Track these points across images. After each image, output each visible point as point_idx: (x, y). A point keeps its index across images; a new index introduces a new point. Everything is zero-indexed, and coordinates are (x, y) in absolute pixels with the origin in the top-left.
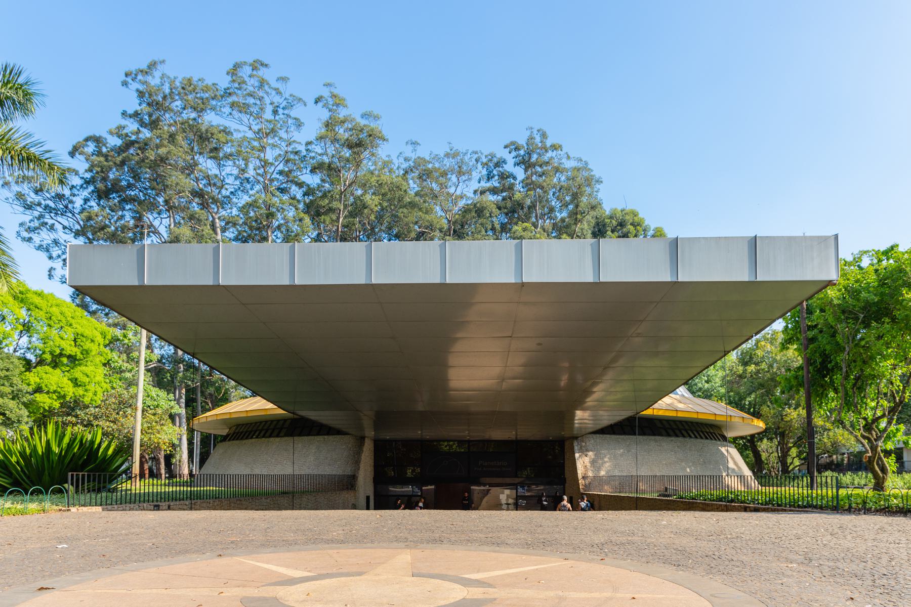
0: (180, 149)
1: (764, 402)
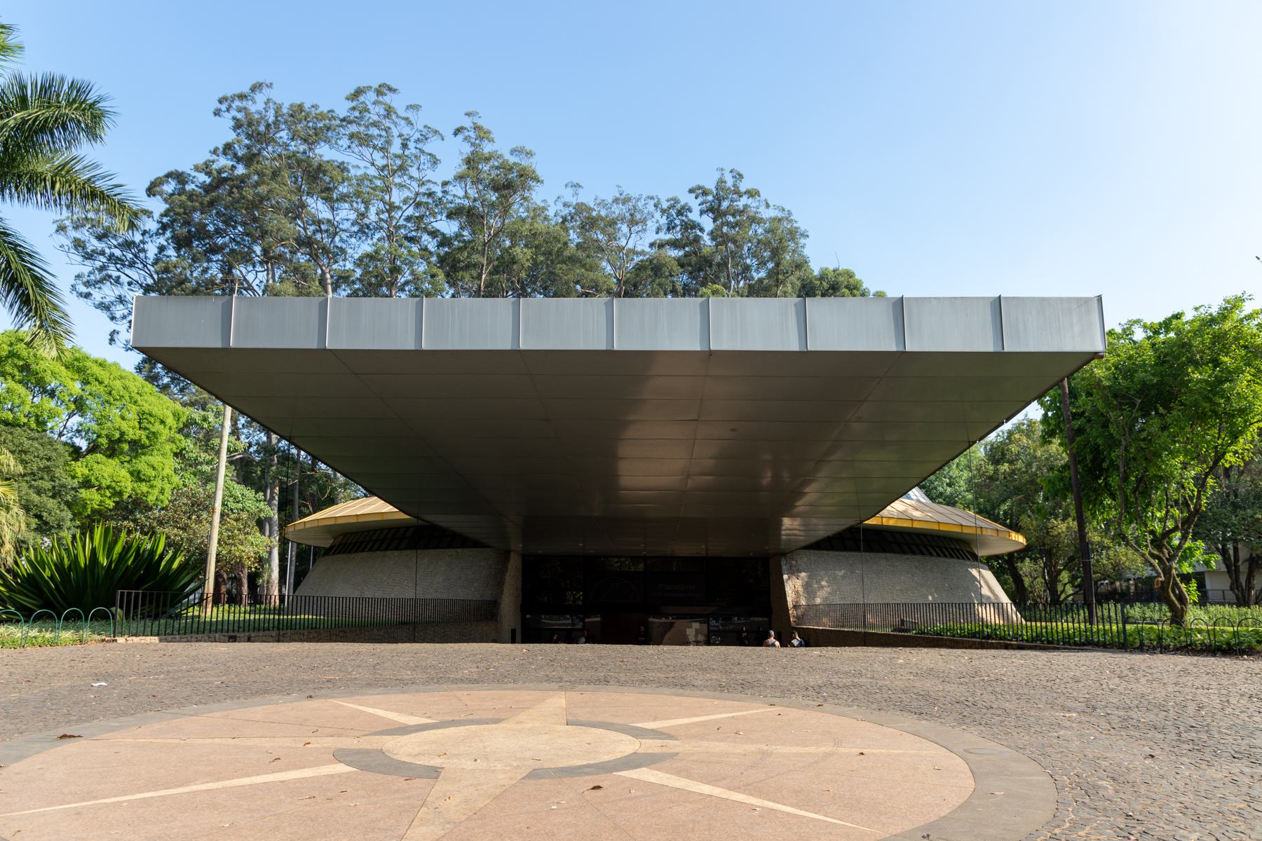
0: (284, 187)
1: (1023, 511)
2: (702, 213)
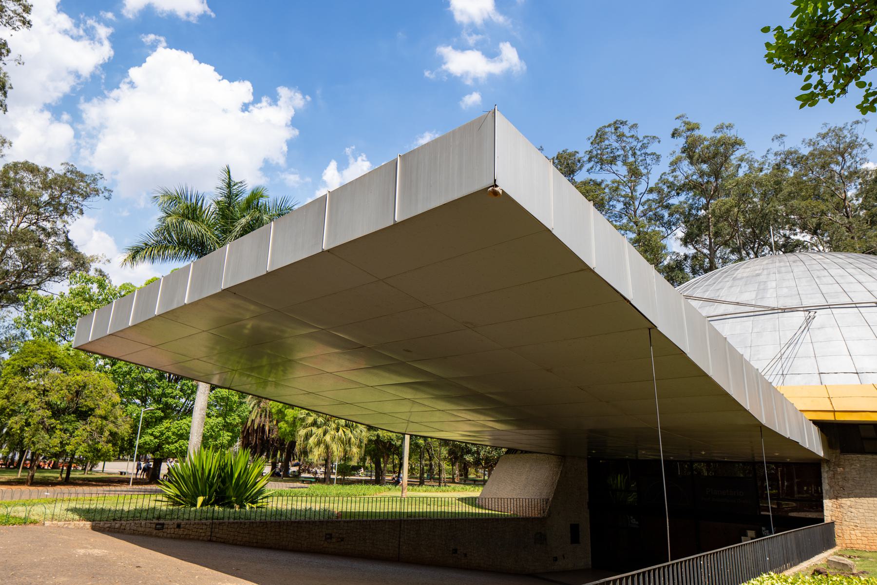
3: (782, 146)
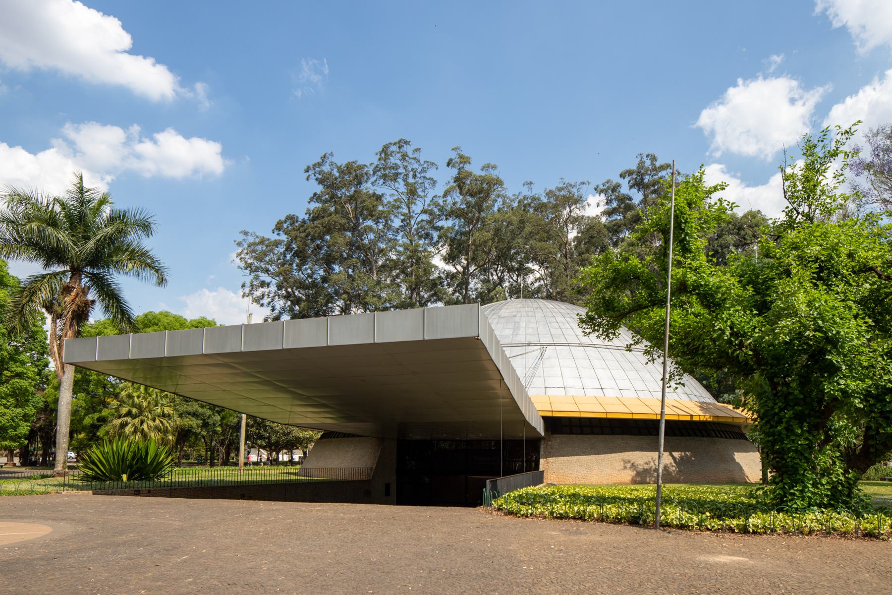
2: (631, 187)
3: (530, 191)
